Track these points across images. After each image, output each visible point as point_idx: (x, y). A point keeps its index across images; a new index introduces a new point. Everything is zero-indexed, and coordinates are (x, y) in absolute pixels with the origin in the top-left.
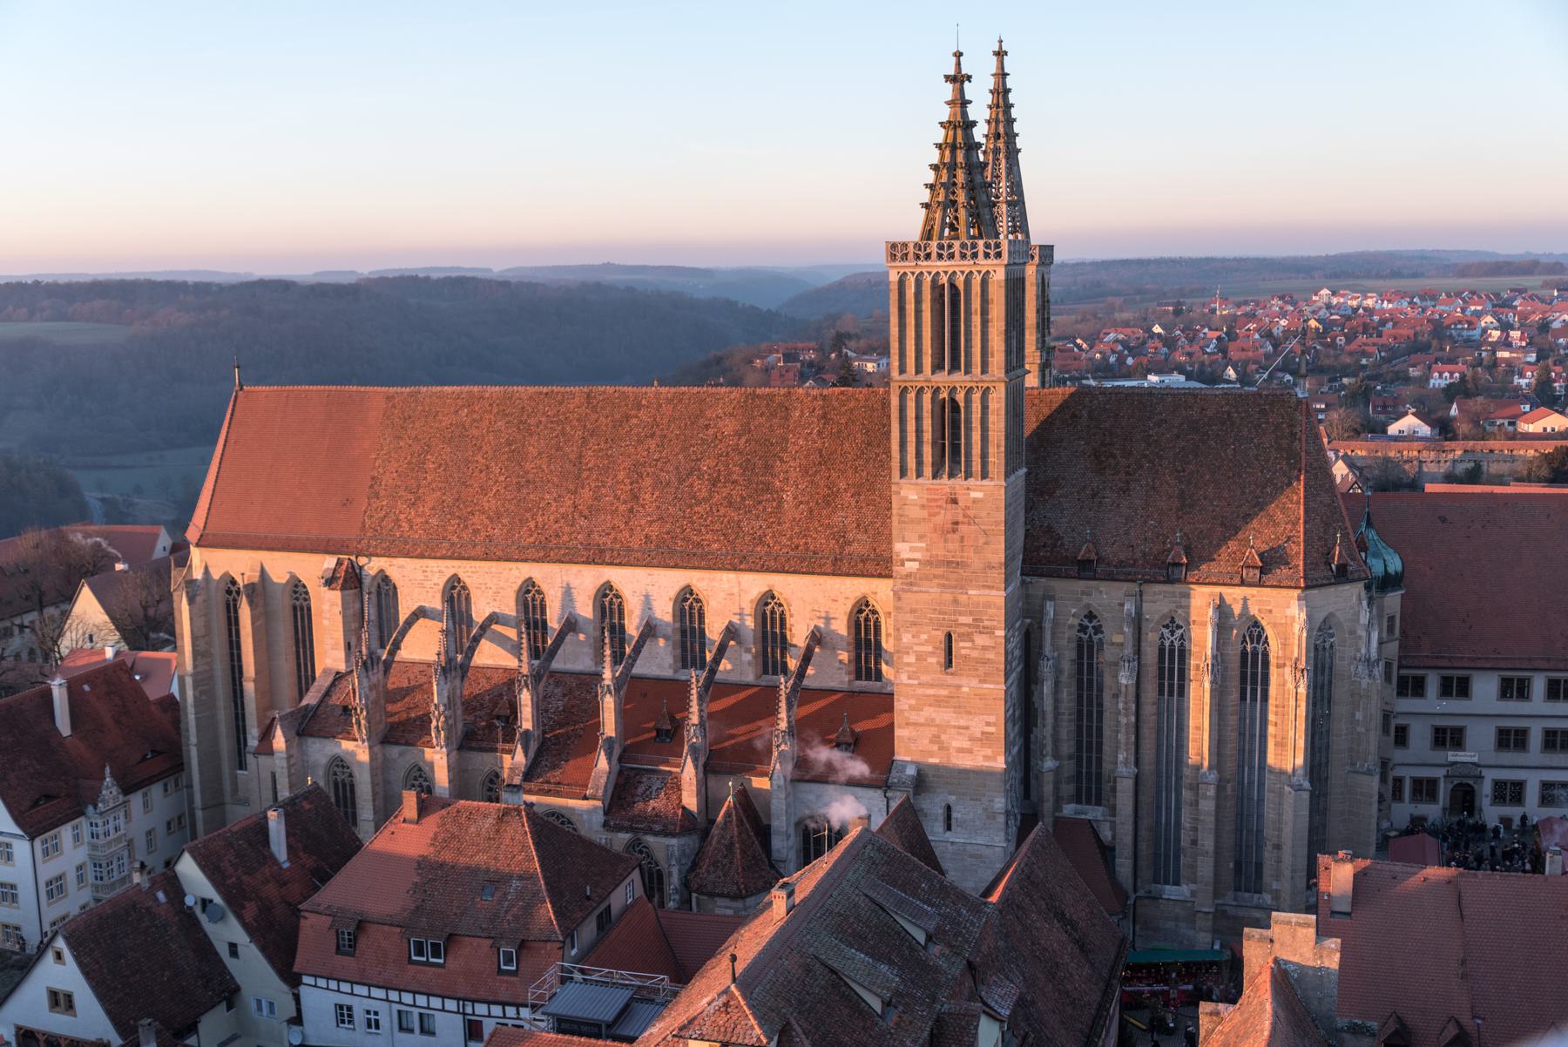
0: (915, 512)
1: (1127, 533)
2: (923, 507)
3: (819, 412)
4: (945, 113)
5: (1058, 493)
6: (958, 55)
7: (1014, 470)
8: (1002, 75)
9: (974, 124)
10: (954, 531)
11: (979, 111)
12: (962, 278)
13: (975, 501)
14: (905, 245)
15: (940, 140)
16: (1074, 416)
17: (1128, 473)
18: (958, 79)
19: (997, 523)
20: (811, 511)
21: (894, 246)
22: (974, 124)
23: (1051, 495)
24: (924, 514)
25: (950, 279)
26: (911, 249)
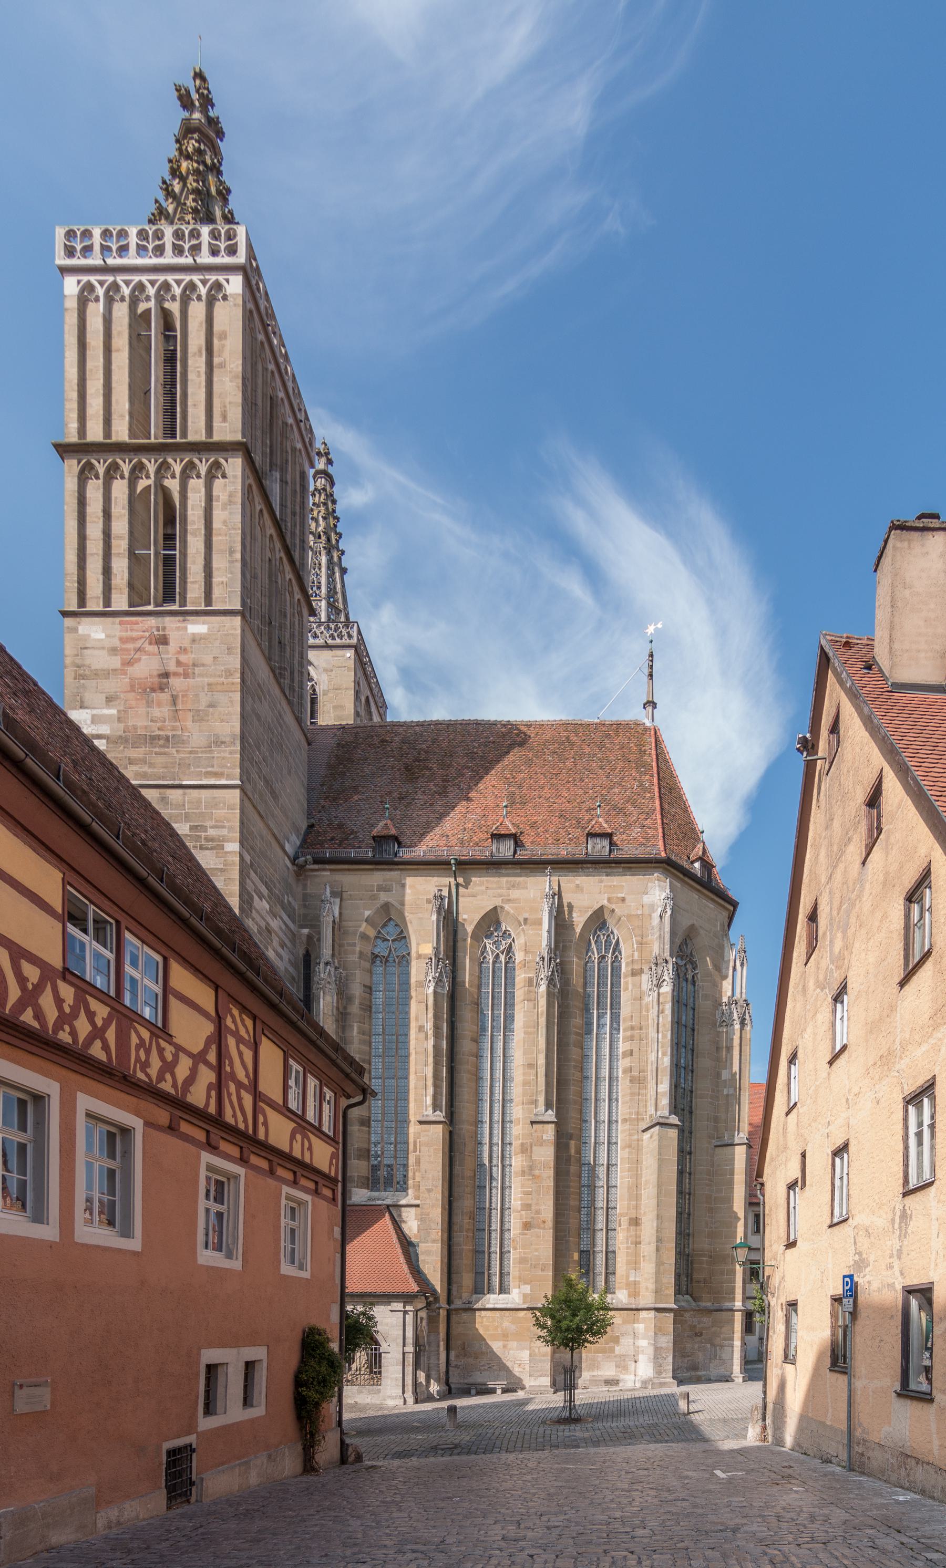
2: (113, 651)
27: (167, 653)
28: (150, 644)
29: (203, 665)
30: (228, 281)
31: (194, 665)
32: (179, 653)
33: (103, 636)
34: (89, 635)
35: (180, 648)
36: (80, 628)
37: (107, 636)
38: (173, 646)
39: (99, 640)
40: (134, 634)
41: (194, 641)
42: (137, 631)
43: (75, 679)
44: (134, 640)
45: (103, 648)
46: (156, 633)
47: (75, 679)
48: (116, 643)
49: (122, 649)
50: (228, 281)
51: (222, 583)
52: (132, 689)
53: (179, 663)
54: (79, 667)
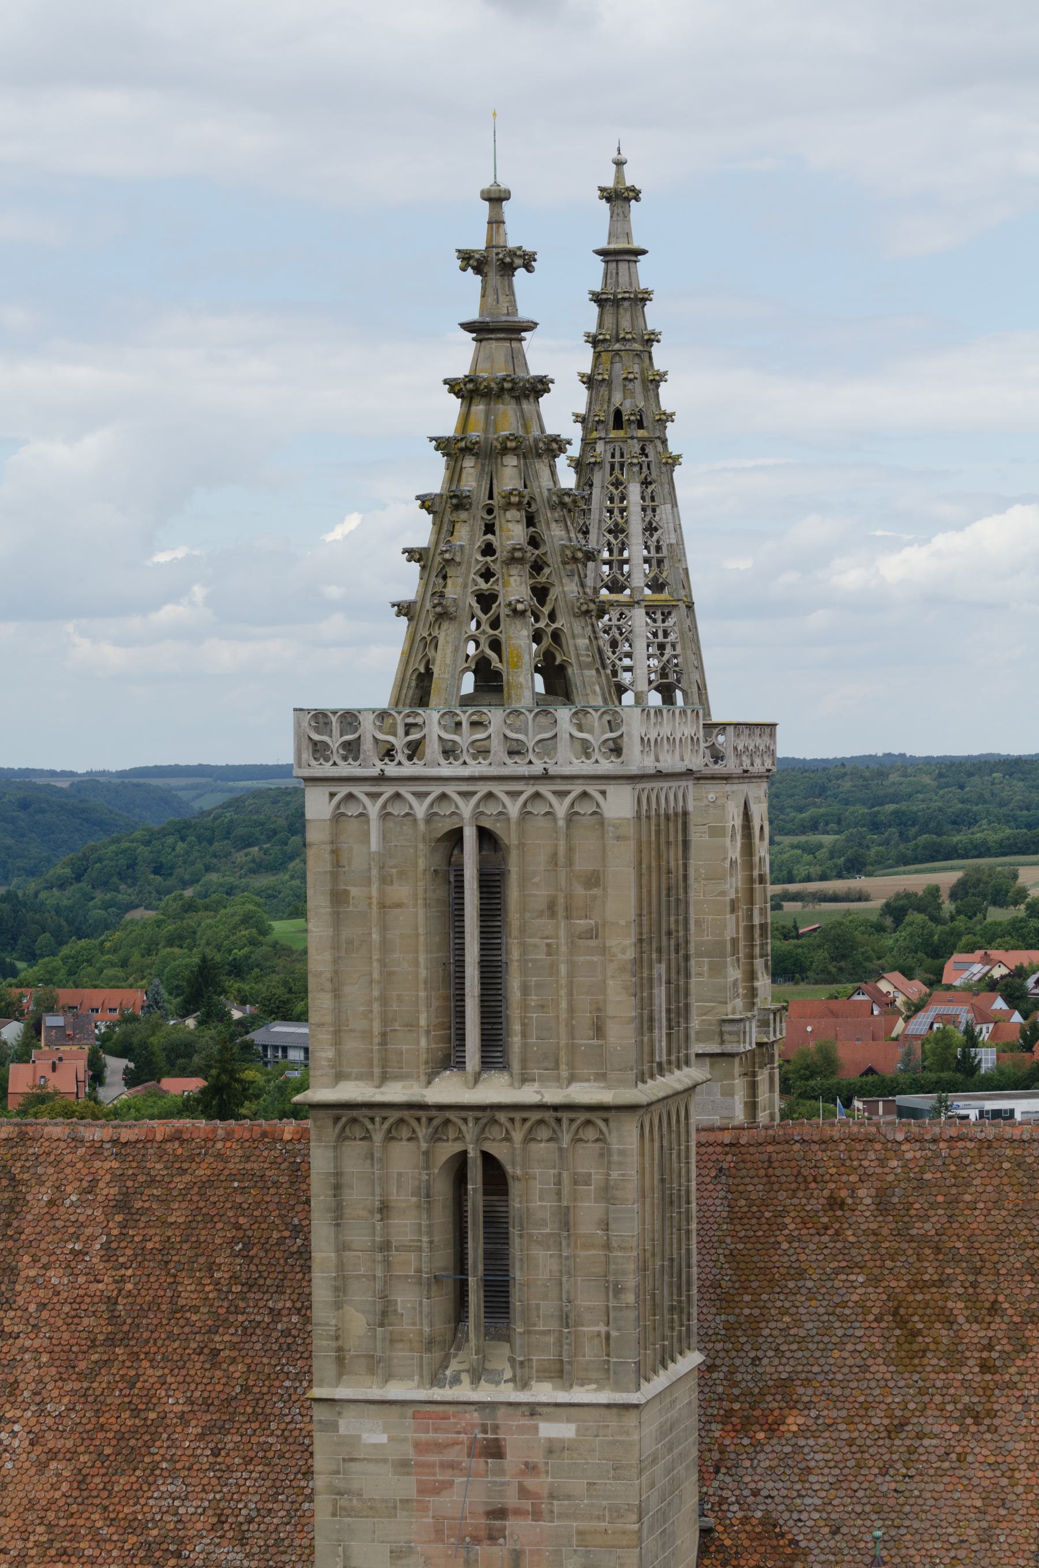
0: (380, 1483)
1: (987, 1537)
2: (403, 1466)
3: (107, 1190)
4: (461, 356)
5: (793, 1422)
6: (496, 198)
7: (665, 1359)
8: (619, 256)
9: (540, 387)
10: (492, 1537)
11: (559, 353)
12: (514, 809)
13: (552, 1448)
14: (350, 718)
15: (448, 429)
16: (834, 1203)
17: (985, 1367)
18: (497, 264)
19: (616, 1513)
20: (81, 1480)
21: (320, 718)
22: (540, 387)
23: (773, 1429)
24: (407, 1486)
25: (478, 814)
26: (368, 727)
27: (502, 1472)
28: (469, 1455)
29: (568, 1497)
30: (603, 793)
31: (552, 1496)
32: (522, 1473)
33: (383, 1439)
34: (359, 1437)
35: (526, 1464)
36: (342, 1423)
37: (390, 1439)
38: (513, 1459)
39: (375, 1446)
40: (441, 1437)
41: (551, 1452)
42: (447, 1431)
43: (334, 1515)
44: (440, 1447)
45: (385, 1461)
46: (480, 1436)
47: (334, 1515)
48: (411, 1453)
49: (419, 1464)
50: (603, 793)
51: (599, 1334)
52: (439, 1534)
53: (524, 1492)
54: (340, 1493)
